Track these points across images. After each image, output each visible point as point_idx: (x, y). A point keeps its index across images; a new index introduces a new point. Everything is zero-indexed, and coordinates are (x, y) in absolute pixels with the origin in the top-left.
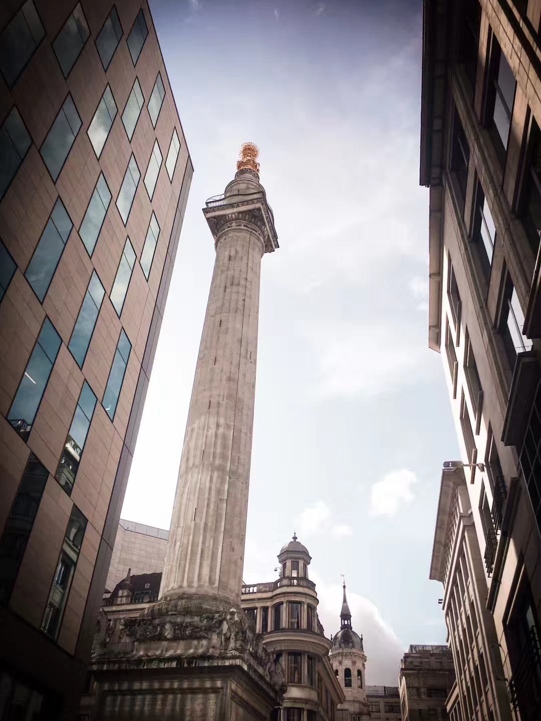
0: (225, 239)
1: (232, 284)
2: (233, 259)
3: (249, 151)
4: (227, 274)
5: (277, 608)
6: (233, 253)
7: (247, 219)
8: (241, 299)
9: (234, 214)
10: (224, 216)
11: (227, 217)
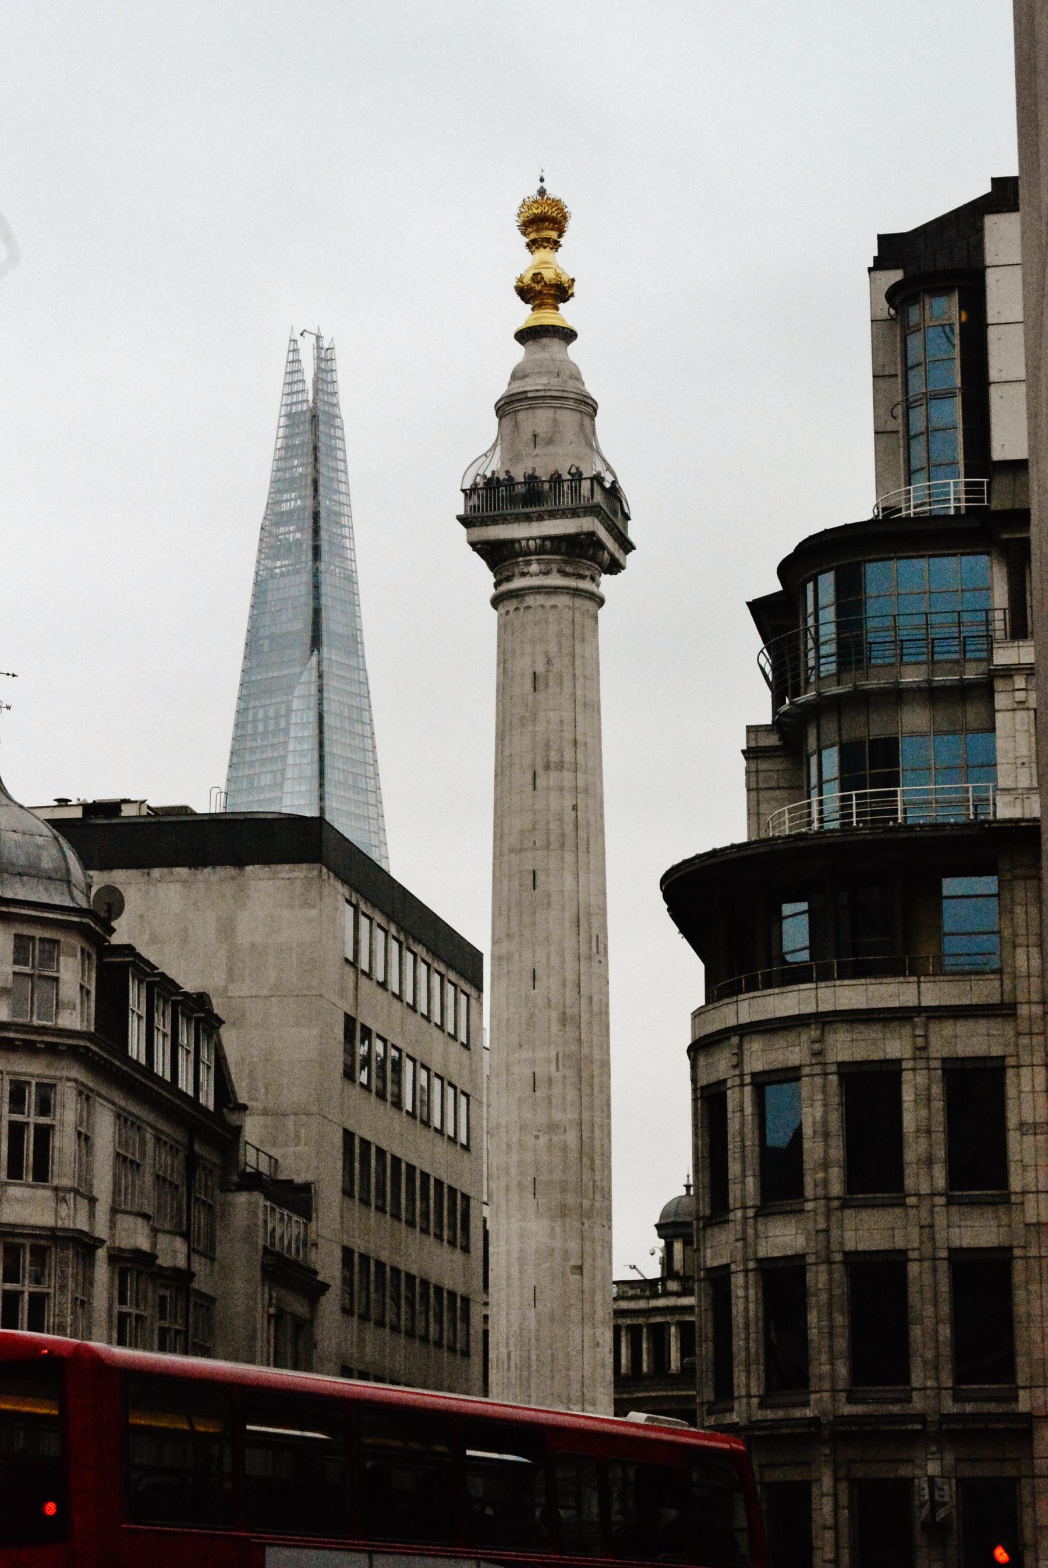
0: (517, 609)
1: (547, 767)
2: (541, 686)
3: (544, 224)
4: (534, 733)
5: (659, 1334)
6: (540, 669)
7: (563, 549)
8: (568, 802)
9: (534, 539)
10: (512, 542)
11: (517, 545)
